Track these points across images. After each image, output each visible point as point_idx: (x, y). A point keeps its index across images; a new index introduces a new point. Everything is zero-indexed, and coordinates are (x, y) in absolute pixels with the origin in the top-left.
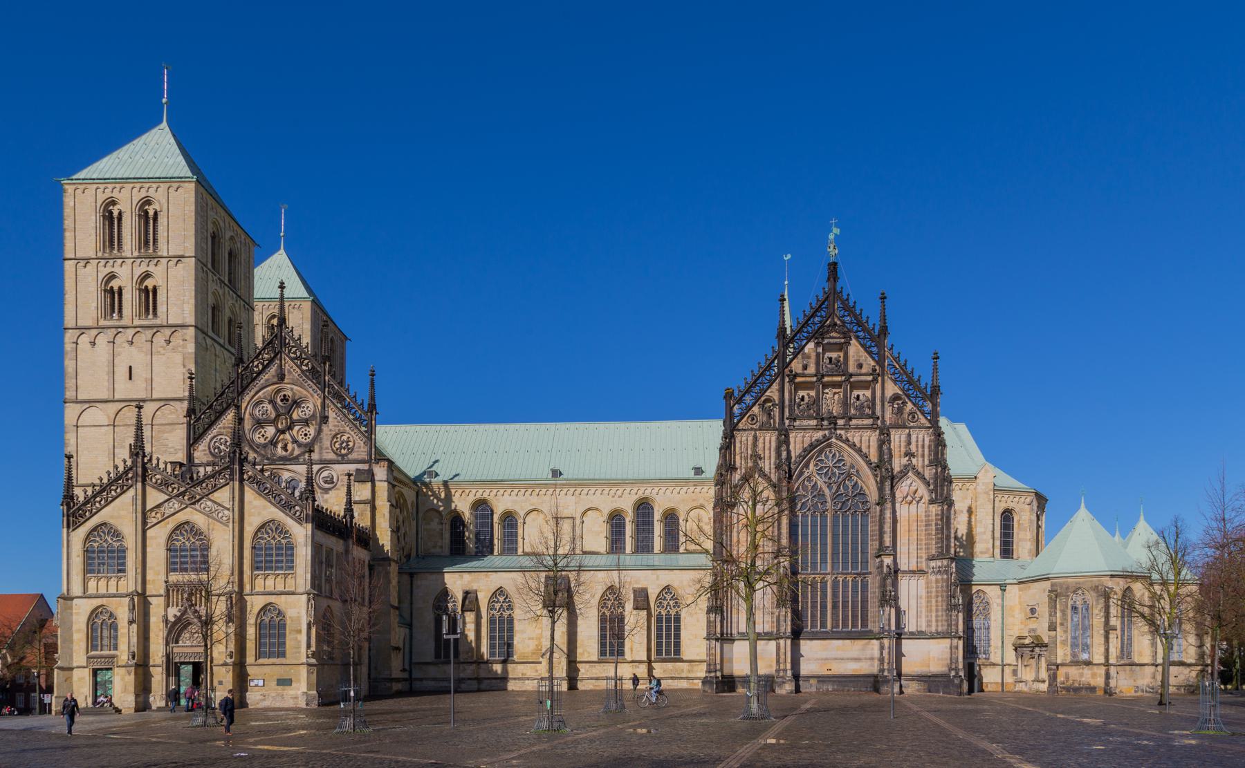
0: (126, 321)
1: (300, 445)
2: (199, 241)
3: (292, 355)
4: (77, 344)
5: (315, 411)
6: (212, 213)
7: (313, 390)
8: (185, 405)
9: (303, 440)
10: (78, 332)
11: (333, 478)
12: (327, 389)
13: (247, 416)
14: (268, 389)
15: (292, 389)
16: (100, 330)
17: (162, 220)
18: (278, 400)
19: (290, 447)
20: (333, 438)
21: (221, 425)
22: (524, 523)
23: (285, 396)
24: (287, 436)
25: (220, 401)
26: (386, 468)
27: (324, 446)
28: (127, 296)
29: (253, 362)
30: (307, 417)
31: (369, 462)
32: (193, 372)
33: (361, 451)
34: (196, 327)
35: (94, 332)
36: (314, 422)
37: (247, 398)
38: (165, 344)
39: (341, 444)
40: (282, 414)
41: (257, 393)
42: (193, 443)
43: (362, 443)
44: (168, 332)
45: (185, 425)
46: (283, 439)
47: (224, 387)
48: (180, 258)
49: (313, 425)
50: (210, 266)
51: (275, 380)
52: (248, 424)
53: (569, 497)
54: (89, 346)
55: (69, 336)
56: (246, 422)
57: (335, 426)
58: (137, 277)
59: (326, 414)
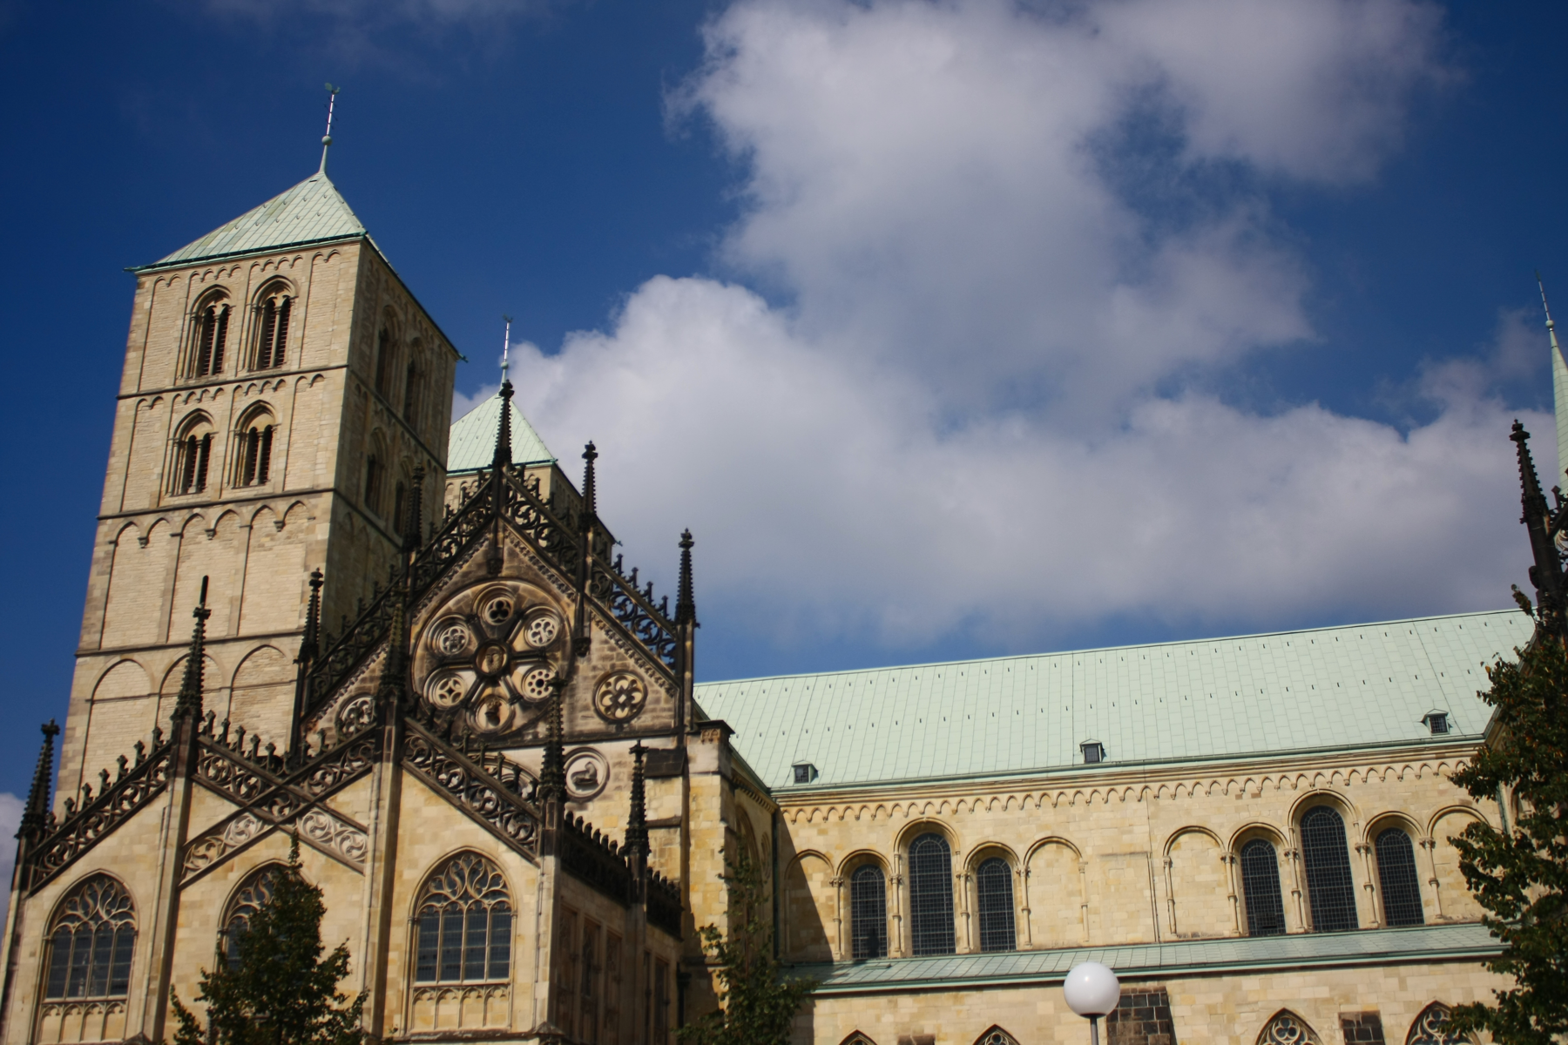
0: (209, 495)
1: (526, 705)
2: (358, 341)
3: (520, 521)
4: (115, 543)
5: (562, 632)
6: (386, 297)
7: (560, 586)
8: (300, 640)
9: (535, 695)
10: (121, 522)
11: (595, 774)
12: (589, 583)
13: (420, 651)
14: (468, 592)
15: (515, 590)
16: (161, 515)
17: (297, 312)
18: (486, 615)
19: (505, 710)
20: (598, 685)
21: (367, 674)
22: (1027, 872)
23: (500, 604)
24: (503, 690)
25: (367, 626)
26: (716, 743)
27: (580, 704)
28: (218, 450)
29: (440, 541)
30: (545, 644)
31: (677, 732)
32: (323, 571)
33: (659, 707)
34: (335, 491)
35: (151, 519)
36: (559, 654)
37: (423, 614)
38: (274, 530)
39: (615, 699)
40: (493, 642)
42: (307, 715)
43: (662, 691)
44: (281, 506)
45: (294, 685)
46: (491, 696)
47: (380, 596)
48: (318, 374)
49: (556, 660)
50: (372, 386)
52: (418, 670)
53: (1132, 805)
54: (137, 545)
55: (105, 531)
56: (417, 664)
57: (605, 658)
58: (239, 413)
59: (586, 635)
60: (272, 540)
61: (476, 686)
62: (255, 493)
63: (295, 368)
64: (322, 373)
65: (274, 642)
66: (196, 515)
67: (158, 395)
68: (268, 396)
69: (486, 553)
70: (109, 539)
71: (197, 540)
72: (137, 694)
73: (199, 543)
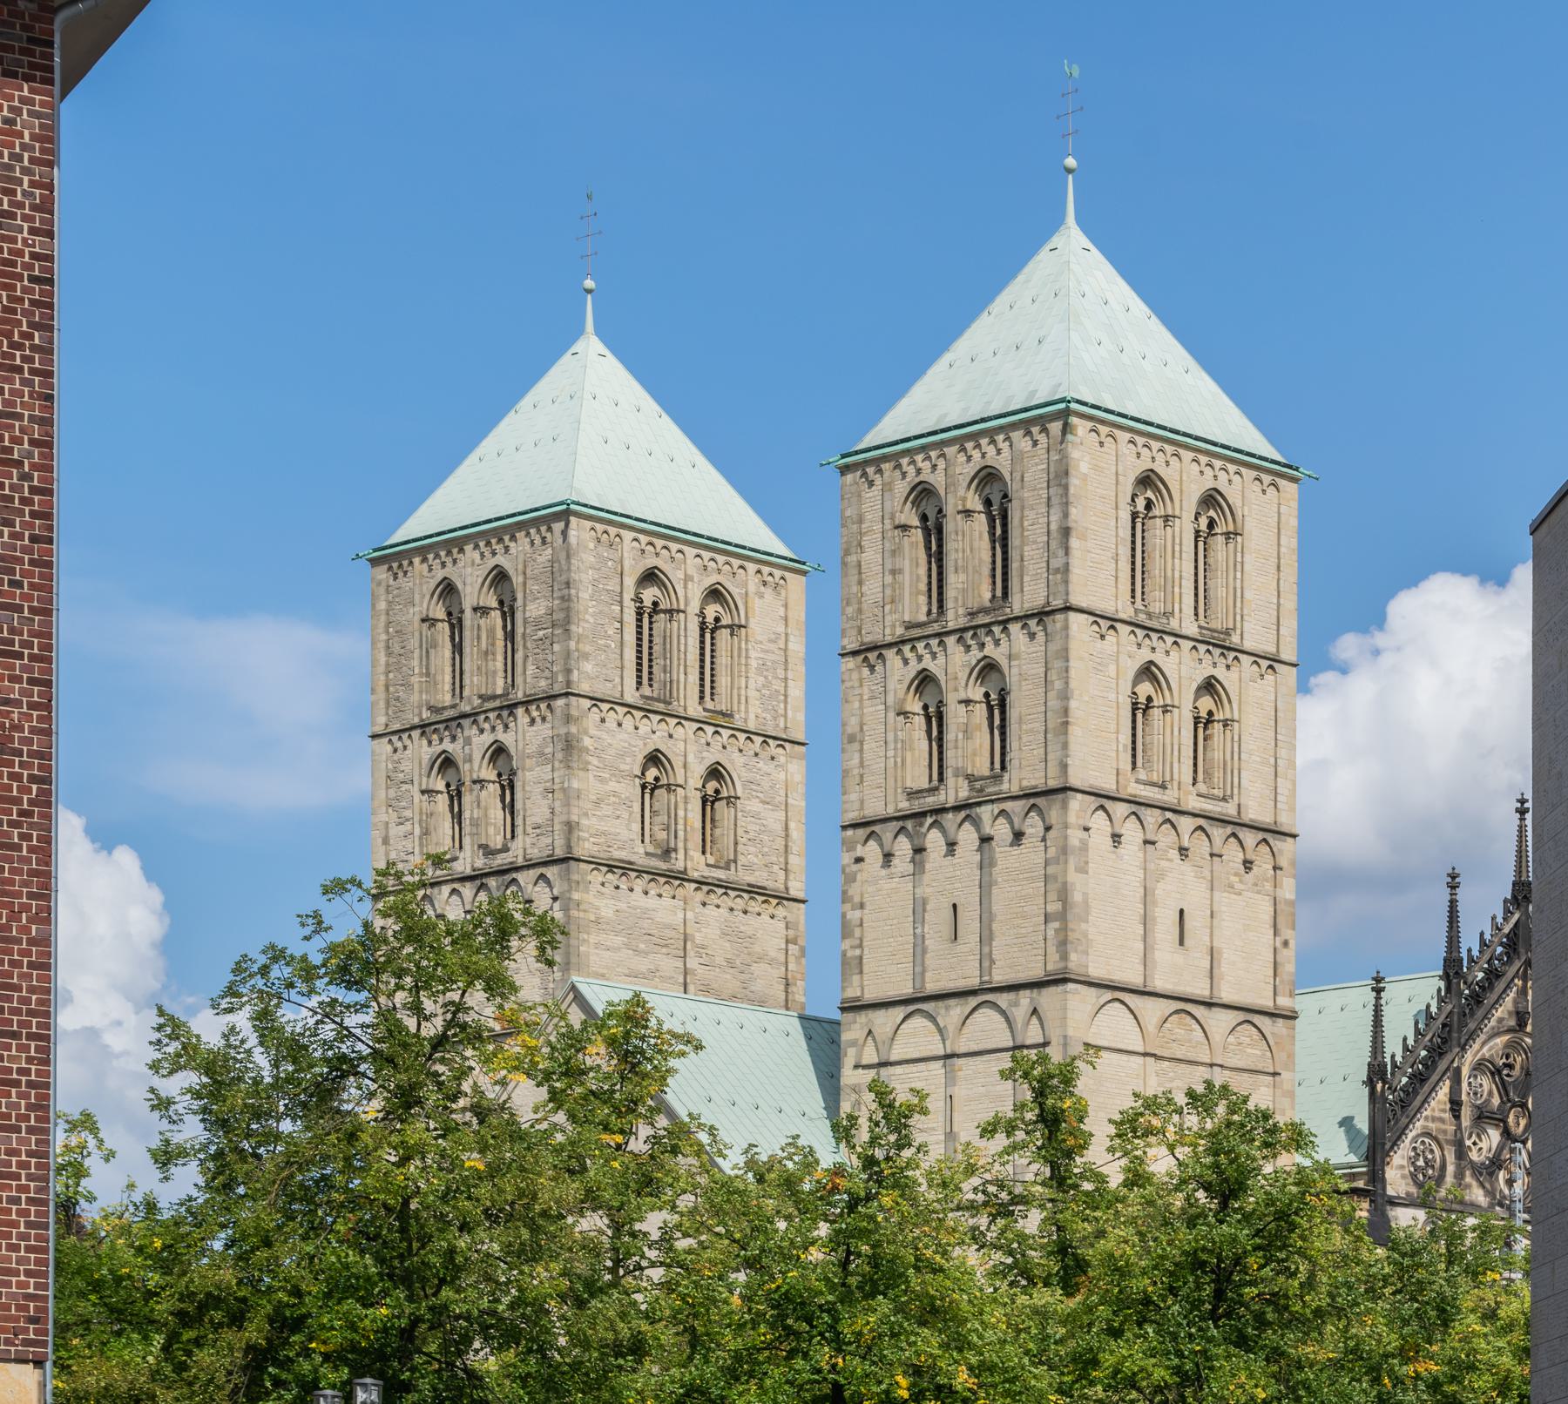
10: (1093, 802)
16: (1134, 808)
41: (1484, 1044)
51: (1512, 1023)
54: (1109, 840)
60: (1241, 881)
61: (1500, 1148)
62: (1219, 809)
63: (1248, 645)
64: (1276, 665)
65: (1257, 1019)
66: (1168, 821)
67: (1113, 622)
68: (1220, 673)
69: (1515, 1002)
70: (1081, 822)
71: (1169, 856)
72: (1130, 1048)
73: (1171, 860)
